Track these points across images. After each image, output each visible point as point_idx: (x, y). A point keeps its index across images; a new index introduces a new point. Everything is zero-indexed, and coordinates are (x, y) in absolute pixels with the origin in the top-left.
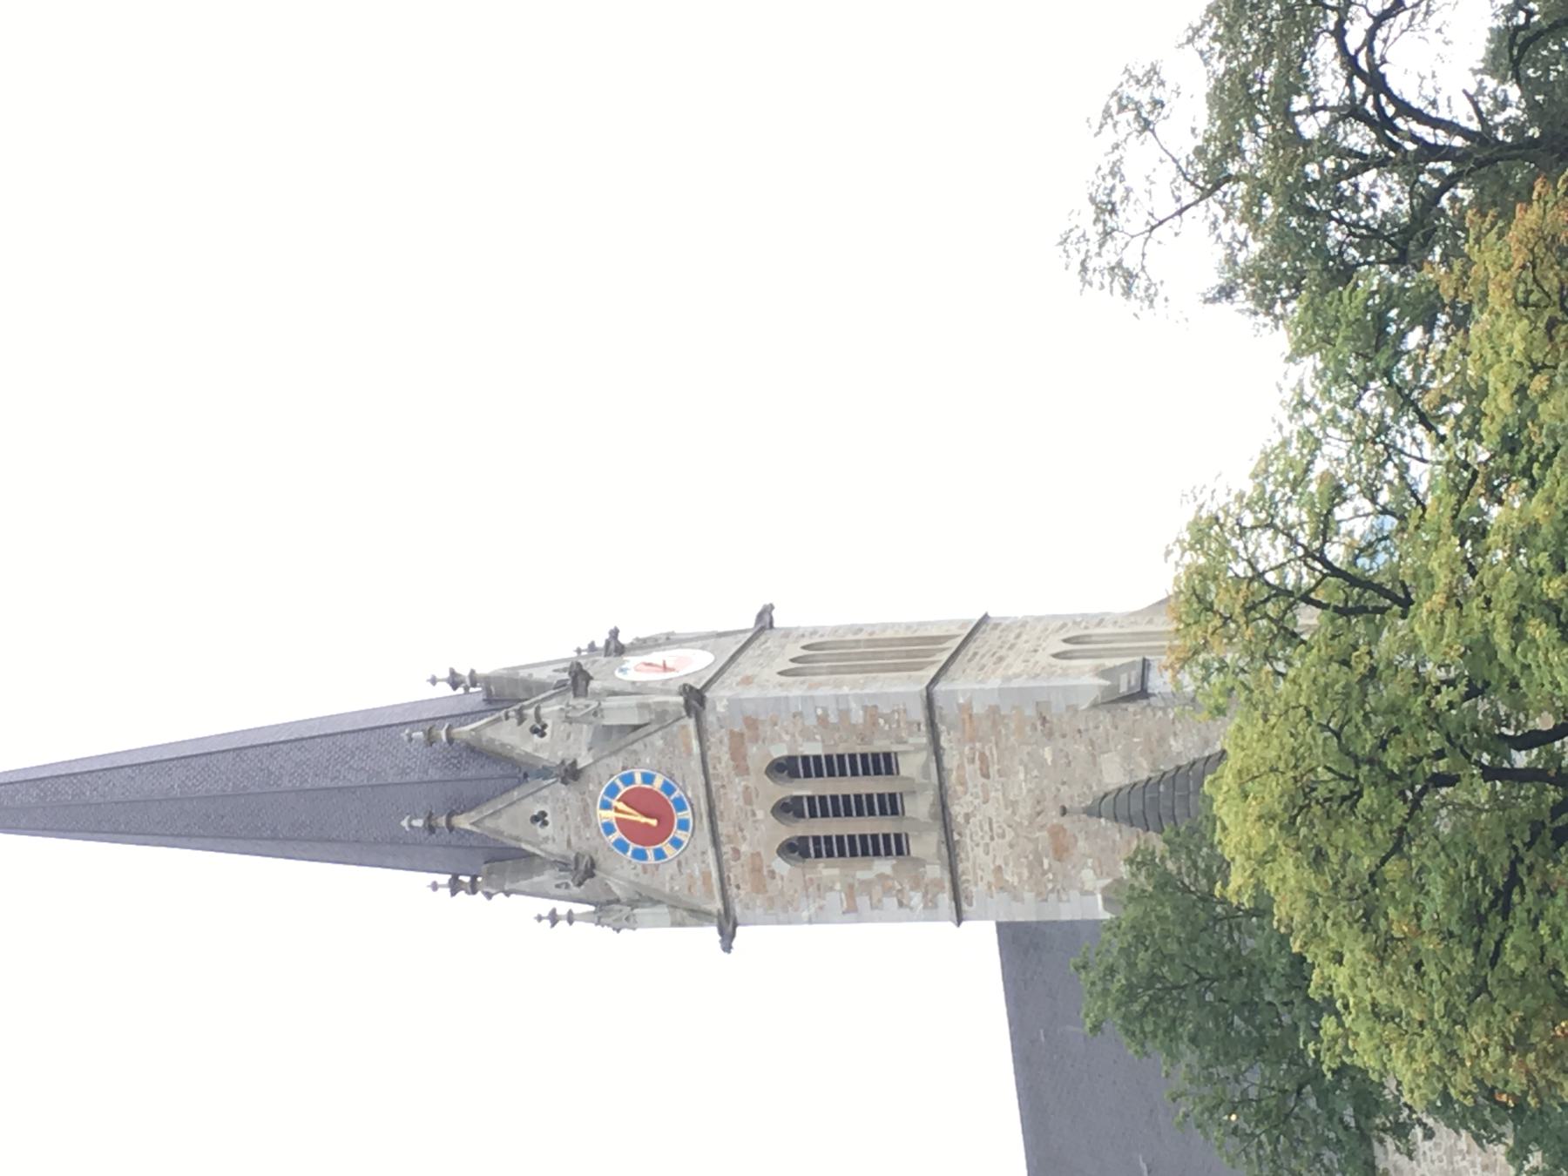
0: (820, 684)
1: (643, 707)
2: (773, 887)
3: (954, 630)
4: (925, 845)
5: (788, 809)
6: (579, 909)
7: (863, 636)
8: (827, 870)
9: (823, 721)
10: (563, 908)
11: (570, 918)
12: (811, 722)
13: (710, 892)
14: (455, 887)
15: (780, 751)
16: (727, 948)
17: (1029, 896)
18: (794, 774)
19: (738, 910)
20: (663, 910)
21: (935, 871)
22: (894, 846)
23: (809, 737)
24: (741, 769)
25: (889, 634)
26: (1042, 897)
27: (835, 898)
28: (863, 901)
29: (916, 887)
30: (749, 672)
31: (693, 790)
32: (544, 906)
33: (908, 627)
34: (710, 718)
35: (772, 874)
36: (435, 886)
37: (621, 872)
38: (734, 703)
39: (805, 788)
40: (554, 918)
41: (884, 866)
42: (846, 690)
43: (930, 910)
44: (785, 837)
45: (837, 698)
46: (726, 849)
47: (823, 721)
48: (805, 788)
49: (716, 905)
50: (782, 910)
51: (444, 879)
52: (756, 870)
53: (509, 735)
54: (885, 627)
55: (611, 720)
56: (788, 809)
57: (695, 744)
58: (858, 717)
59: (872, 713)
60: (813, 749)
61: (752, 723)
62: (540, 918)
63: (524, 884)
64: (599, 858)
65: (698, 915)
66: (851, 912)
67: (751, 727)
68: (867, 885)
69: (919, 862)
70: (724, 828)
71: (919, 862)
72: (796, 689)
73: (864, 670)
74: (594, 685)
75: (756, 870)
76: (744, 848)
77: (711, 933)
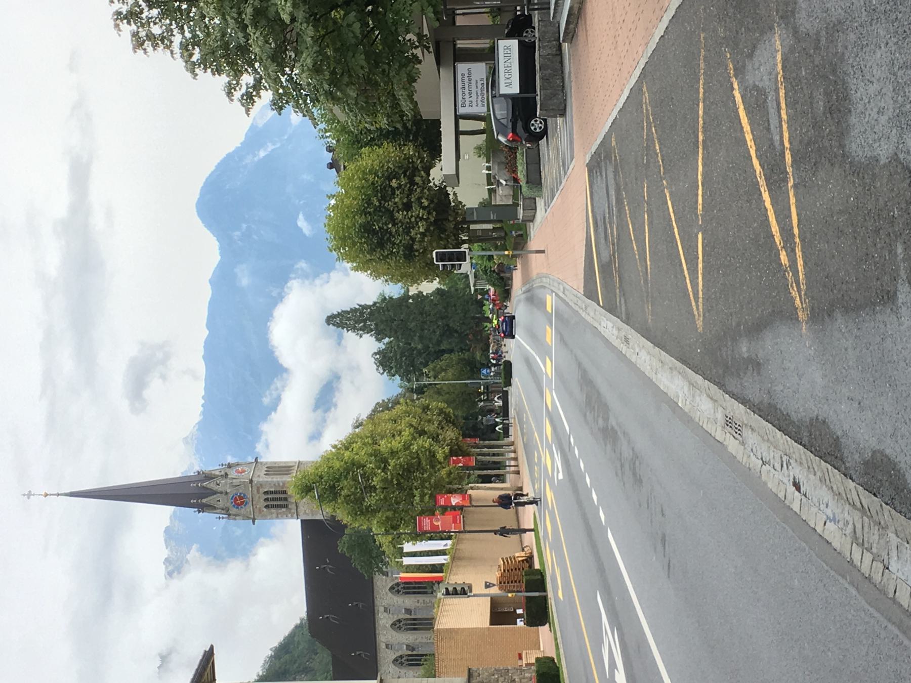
0: (273, 478)
1: (240, 482)
2: (263, 513)
3: (294, 464)
4: (293, 507)
5: (266, 500)
6: (224, 516)
7: (276, 465)
8: (273, 510)
9: (275, 485)
10: (221, 516)
11: (223, 518)
12: (272, 485)
13: (251, 514)
14: (199, 512)
15: (266, 490)
16: (254, 524)
17: (310, 515)
18: (268, 494)
19: (256, 517)
20: (241, 517)
21: (294, 511)
22: (286, 506)
23: (271, 487)
24: (258, 491)
25: (281, 465)
26: (313, 515)
27: (274, 515)
28: (279, 516)
29: (290, 513)
30: (259, 474)
31: (250, 496)
32: (218, 515)
33: (285, 463)
34: (253, 484)
35: (263, 511)
36: (195, 512)
37: (233, 511)
38: (258, 482)
39: (270, 496)
40: (220, 518)
41: (284, 510)
42: (279, 480)
43: (292, 517)
44: (266, 504)
45: (278, 481)
46: (254, 507)
47: (275, 485)
48: (270, 496)
49: (252, 516)
50: (264, 517)
51: (196, 509)
52: (260, 510)
53: (211, 485)
54: (281, 462)
55: (234, 484)
56: (266, 500)
57: (250, 489)
58: (281, 484)
59: (284, 484)
60: (271, 490)
61: (261, 485)
62: (217, 518)
63: (215, 511)
64: (230, 508)
65: (249, 518)
66: (277, 517)
67: (261, 485)
68: (280, 513)
69: (291, 509)
70: (254, 503)
71: (291, 509)
72: (269, 479)
73: (280, 474)
74: (229, 476)
75: (260, 511)
76: (258, 506)
77: (251, 521)
